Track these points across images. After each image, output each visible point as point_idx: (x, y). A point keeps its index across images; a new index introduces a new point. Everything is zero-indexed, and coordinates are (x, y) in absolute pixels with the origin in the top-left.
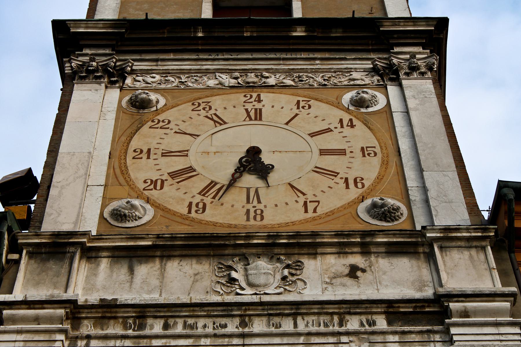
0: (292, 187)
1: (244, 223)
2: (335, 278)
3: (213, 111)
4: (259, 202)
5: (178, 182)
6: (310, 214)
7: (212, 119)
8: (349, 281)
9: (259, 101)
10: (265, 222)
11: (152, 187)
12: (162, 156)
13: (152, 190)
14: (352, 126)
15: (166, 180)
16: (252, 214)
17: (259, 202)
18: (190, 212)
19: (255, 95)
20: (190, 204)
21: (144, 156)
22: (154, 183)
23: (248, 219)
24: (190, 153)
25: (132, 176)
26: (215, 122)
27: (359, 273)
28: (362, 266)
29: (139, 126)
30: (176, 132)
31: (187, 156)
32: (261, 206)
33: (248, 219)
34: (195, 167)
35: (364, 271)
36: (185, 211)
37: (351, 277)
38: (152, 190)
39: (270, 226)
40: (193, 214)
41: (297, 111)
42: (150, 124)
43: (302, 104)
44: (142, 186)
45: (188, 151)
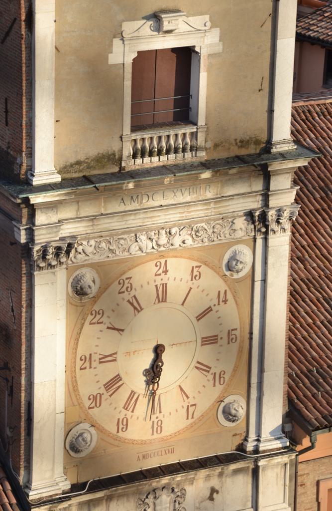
0: (182, 389)
1: (150, 437)
2: (202, 502)
3: (133, 293)
4: (160, 412)
5: (111, 396)
6: (190, 421)
7: (132, 304)
8: (208, 503)
9: (166, 272)
10: (164, 434)
11: (93, 404)
12: (100, 363)
13: (93, 408)
14: (225, 301)
15: (103, 394)
16: (156, 426)
17: (160, 412)
18: (118, 432)
19: (163, 261)
20: (119, 419)
21: (87, 364)
22: (95, 398)
23: (153, 434)
24: (118, 356)
25: (81, 394)
26: (135, 308)
27: (215, 495)
28: (217, 488)
29: (83, 322)
30: (108, 328)
31: (115, 360)
32: (161, 417)
33: (153, 434)
34: (122, 375)
35: (217, 492)
36: (114, 431)
37: (210, 500)
38: (93, 408)
39: (165, 438)
40: (121, 434)
41: (190, 284)
42: (90, 318)
43: (195, 273)
44: (87, 403)
45: (116, 353)
